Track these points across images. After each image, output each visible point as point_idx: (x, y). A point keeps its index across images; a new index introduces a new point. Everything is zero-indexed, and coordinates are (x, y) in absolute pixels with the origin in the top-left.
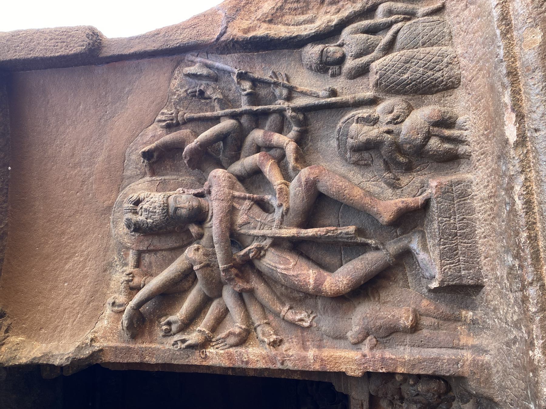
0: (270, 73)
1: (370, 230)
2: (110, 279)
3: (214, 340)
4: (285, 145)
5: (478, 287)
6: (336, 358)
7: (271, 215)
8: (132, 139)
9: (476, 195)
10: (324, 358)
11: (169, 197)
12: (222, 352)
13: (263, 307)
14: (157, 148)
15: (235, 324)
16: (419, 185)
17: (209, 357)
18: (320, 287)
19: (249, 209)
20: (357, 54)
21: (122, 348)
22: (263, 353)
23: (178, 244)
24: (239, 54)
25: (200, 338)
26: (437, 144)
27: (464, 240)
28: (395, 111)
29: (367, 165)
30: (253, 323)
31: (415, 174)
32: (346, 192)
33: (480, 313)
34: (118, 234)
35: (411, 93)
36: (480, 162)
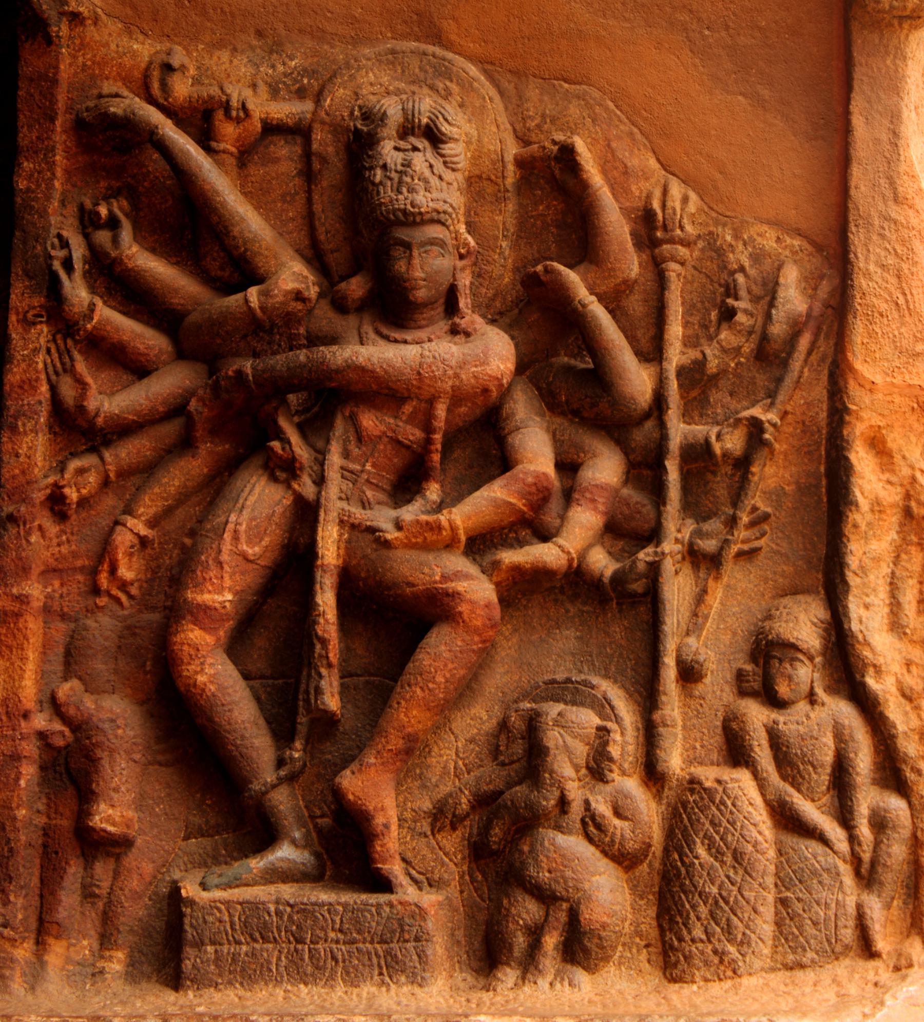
0: (764, 507)
1: (330, 753)
2: (235, 49)
3: (69, 342)
4: (560, 541)
5: (175, 979)
6: (23, 649)
7: (382, 496)
8: (625, 107)
9: (388, 990)
10: (21, 620)
11: (443, 224)
12: (41, 366)
13: (148, 470)
14: (584, 186)
15: (110, 400)
16: (436, 877)
17: (27, 331)
18: (189, 617)
19: (398, 442)
20: (779, 737)
21: (53, 101)
22: (36, 471)
23: (322, 237)
24: (823, 424)
25: (76, 310)
26: (524, 916)
27: (286, 957)
28: (617, 822)
29: (495, 752)
30: (107, 443)
31: (465, 868)
32: (418, 691)
33: (118, 986)
34: (359, 68)
35: (665, 865)
36: (464, 1003)
